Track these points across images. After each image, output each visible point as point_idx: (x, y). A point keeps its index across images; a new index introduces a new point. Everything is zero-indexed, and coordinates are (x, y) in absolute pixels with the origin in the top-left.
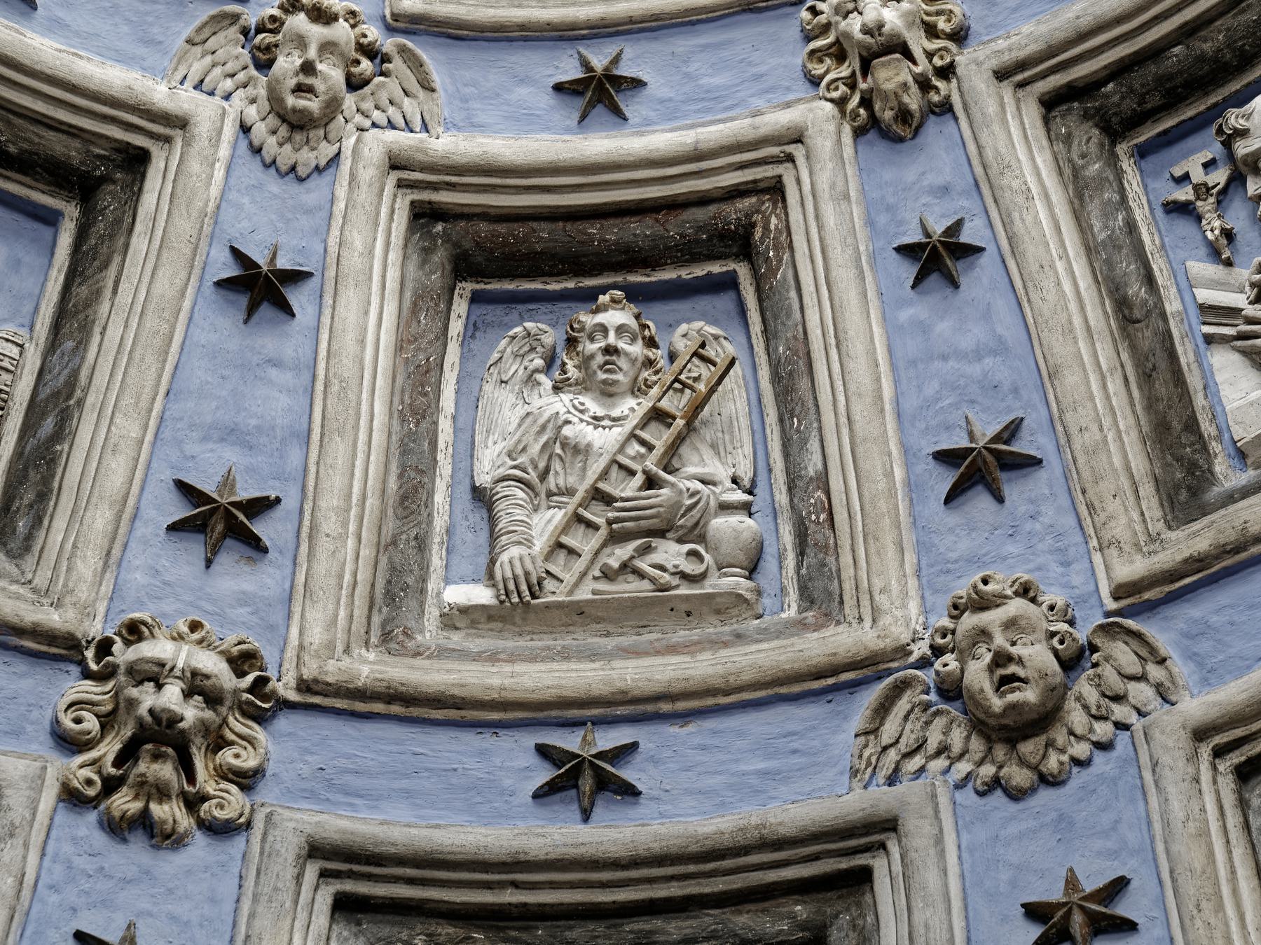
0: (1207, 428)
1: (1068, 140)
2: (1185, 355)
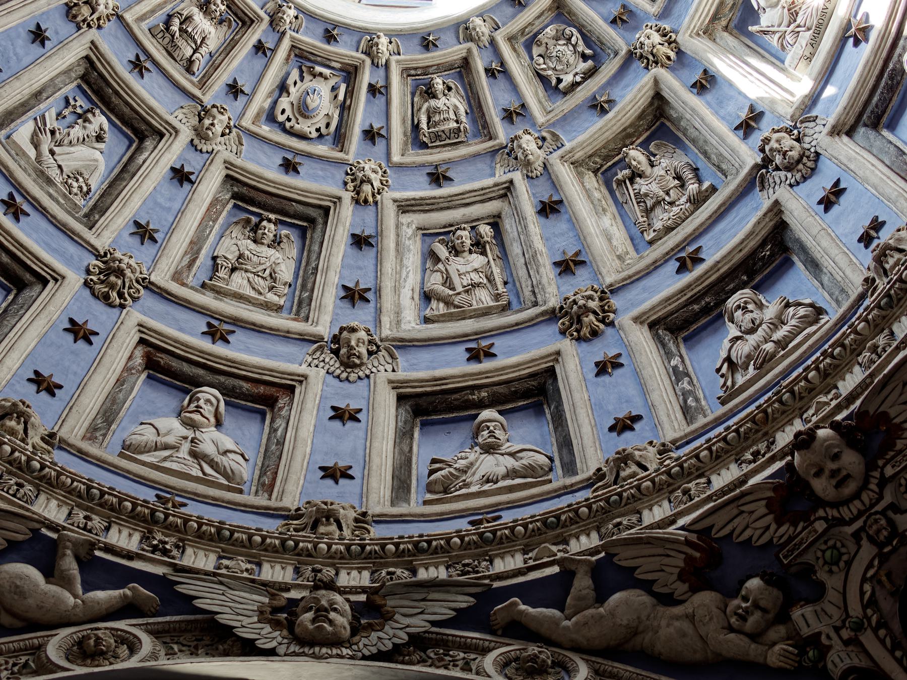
0: (12, 125)
1: (79, 65)
2: (30, 114)
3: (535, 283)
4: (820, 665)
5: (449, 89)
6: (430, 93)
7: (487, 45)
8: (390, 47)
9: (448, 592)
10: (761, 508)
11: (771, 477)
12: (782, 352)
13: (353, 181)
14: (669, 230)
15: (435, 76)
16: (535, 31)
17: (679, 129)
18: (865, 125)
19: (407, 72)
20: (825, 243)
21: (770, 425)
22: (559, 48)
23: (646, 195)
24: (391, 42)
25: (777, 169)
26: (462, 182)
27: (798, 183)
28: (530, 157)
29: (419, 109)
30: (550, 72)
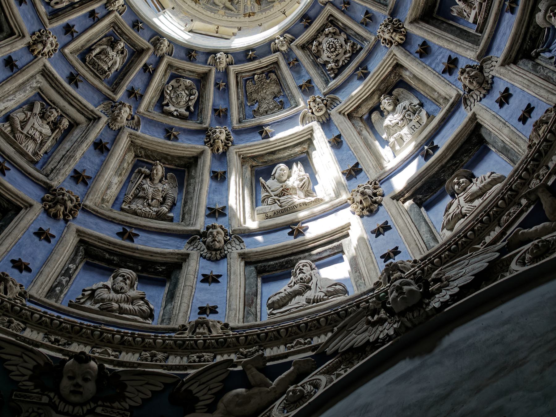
3: (57, 167)
5: (122, 53)
6: (113, 44)
7: (158, 56)
8: (120, 7)
10: (31, 364)
12: (117, 314)
13: (38, 37)
14: (135, 213)
15: (123, 41)
16: (183, 75)
17: (188, 181)
18: (256, 268)
19: (114, 24)
20: (187, 293)
22: (183, 92)
23: (144, 189)
24: (123, 6)
25: (204, 242)
26: (80, 94)
27: (205, 258)
28: (119, 118)
29: (100, 45)
30: (168, 97)
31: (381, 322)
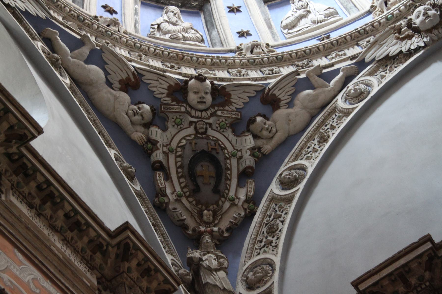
4: (149, 152)
9: (37, 5)
10: (166, 86)
11: (177, 79)
12: (183, 41)
21: (181, 62)
31: (409, 37)
